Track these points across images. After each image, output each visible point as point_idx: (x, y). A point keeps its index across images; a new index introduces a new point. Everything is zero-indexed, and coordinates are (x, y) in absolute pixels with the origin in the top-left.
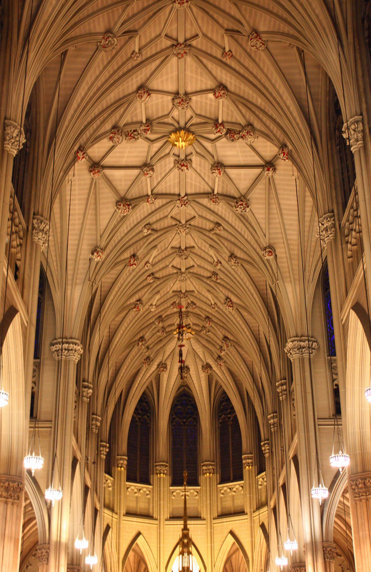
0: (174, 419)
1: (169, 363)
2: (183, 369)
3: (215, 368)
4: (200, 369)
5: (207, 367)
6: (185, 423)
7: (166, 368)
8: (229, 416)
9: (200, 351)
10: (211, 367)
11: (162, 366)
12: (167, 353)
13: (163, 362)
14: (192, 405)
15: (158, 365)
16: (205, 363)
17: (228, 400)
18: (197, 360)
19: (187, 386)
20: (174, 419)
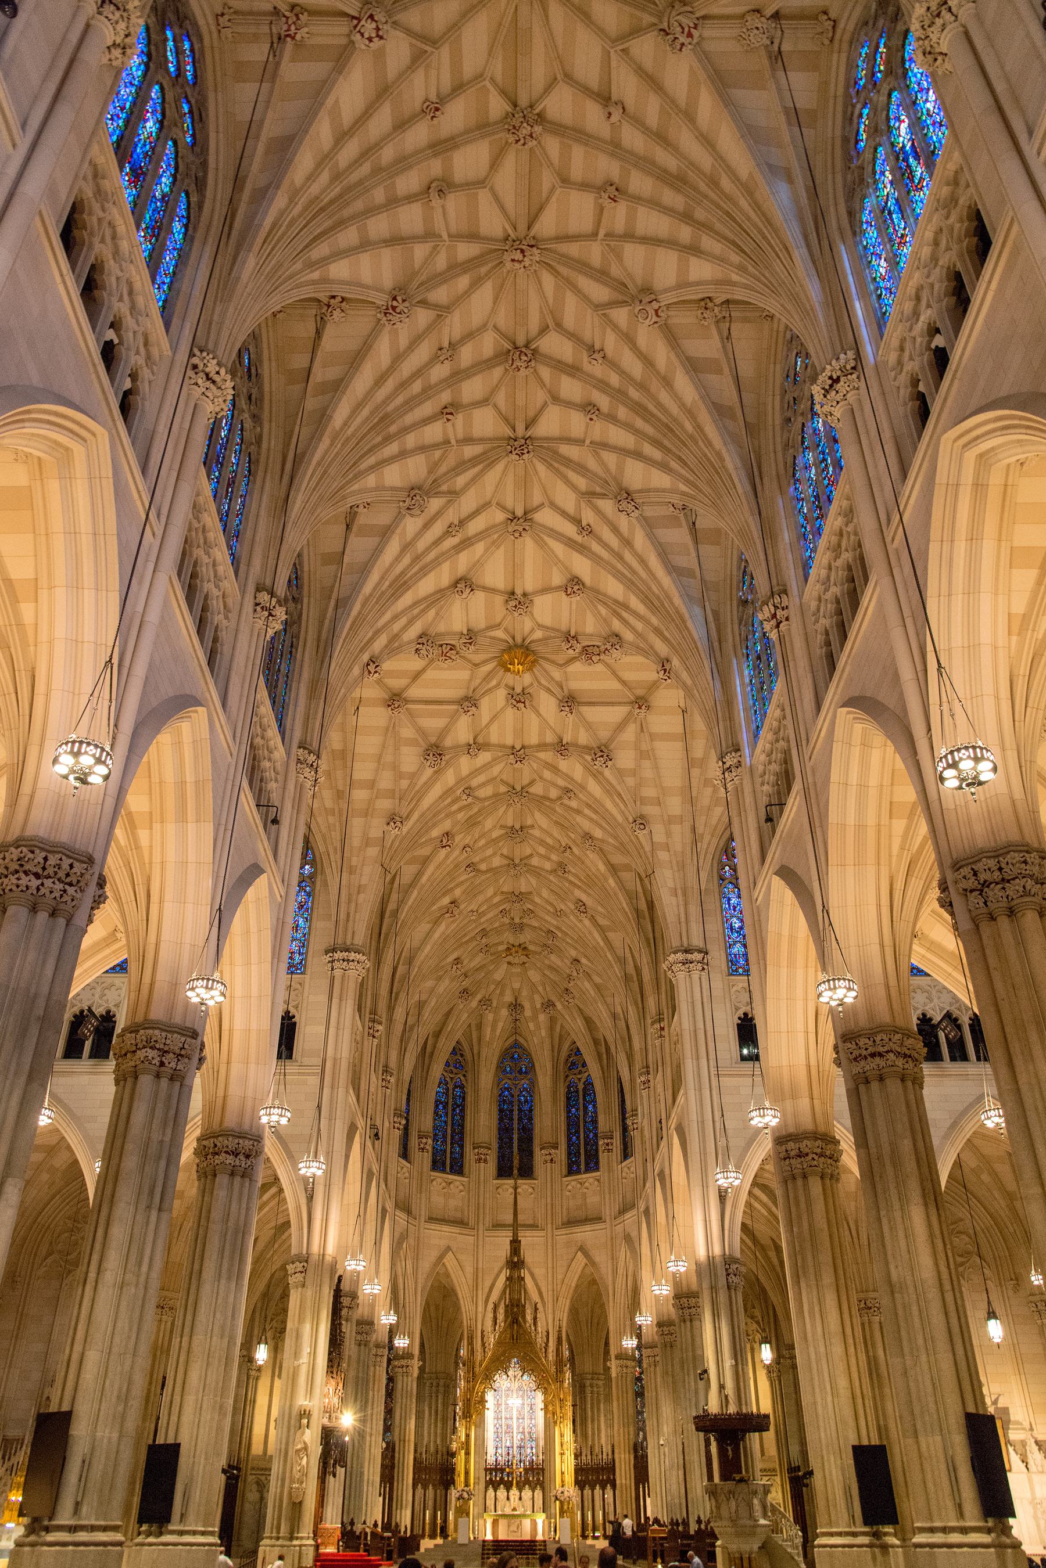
10: (554, 1005)
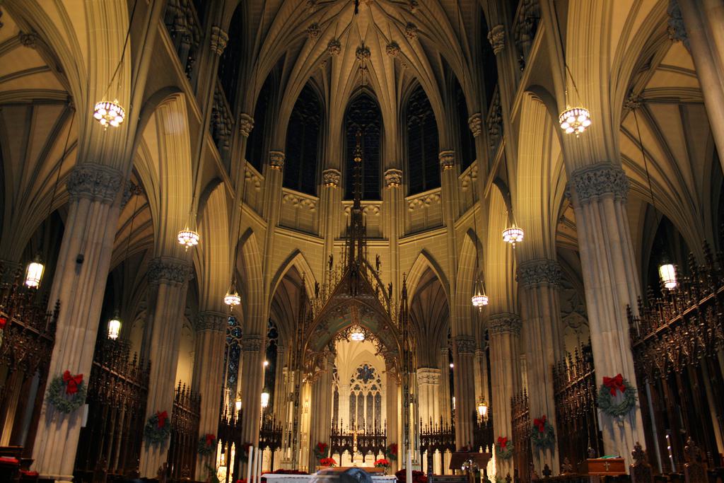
0: (350, 124)
1: (343, 43)
2: (363, 51)
3: (404, 48)
4: (384, 49)
5: (393, 45)
6: (363, 128)
7: (339, 46)
8: (421, 116)
9: (382, 22)
10: (398, 48)
11: (335, 44)
12: (341, 29)
13: (336, 39)
14: (373, 109)
15: (329, 45)
16: (390, 42)
17: (423, 95)
18: (380, 36)
19: (369, 87)
20: (350, 124)
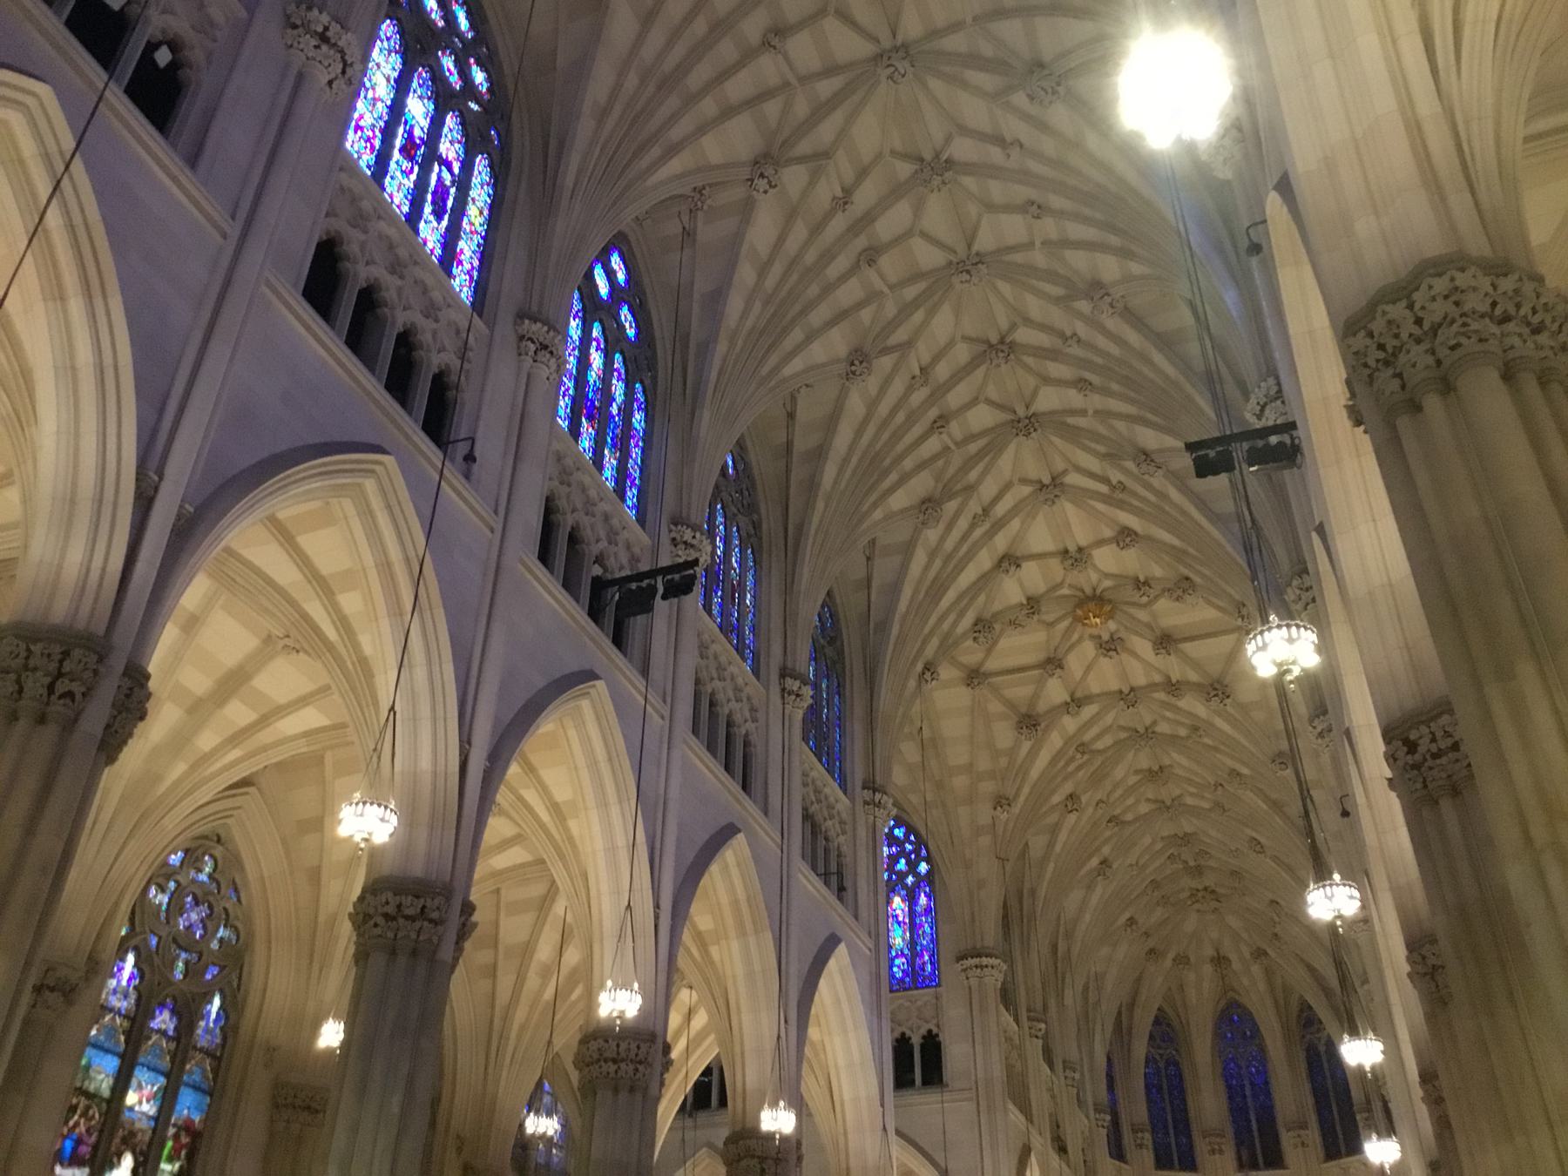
10: (1266, 954)
15: (1174, 960)
